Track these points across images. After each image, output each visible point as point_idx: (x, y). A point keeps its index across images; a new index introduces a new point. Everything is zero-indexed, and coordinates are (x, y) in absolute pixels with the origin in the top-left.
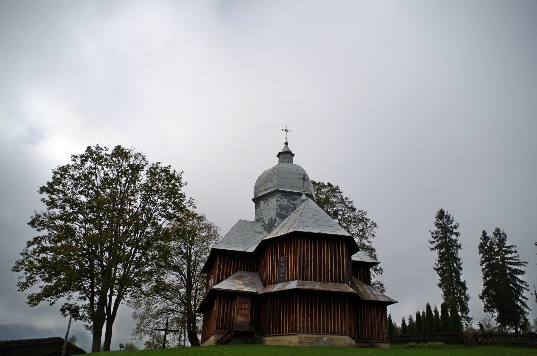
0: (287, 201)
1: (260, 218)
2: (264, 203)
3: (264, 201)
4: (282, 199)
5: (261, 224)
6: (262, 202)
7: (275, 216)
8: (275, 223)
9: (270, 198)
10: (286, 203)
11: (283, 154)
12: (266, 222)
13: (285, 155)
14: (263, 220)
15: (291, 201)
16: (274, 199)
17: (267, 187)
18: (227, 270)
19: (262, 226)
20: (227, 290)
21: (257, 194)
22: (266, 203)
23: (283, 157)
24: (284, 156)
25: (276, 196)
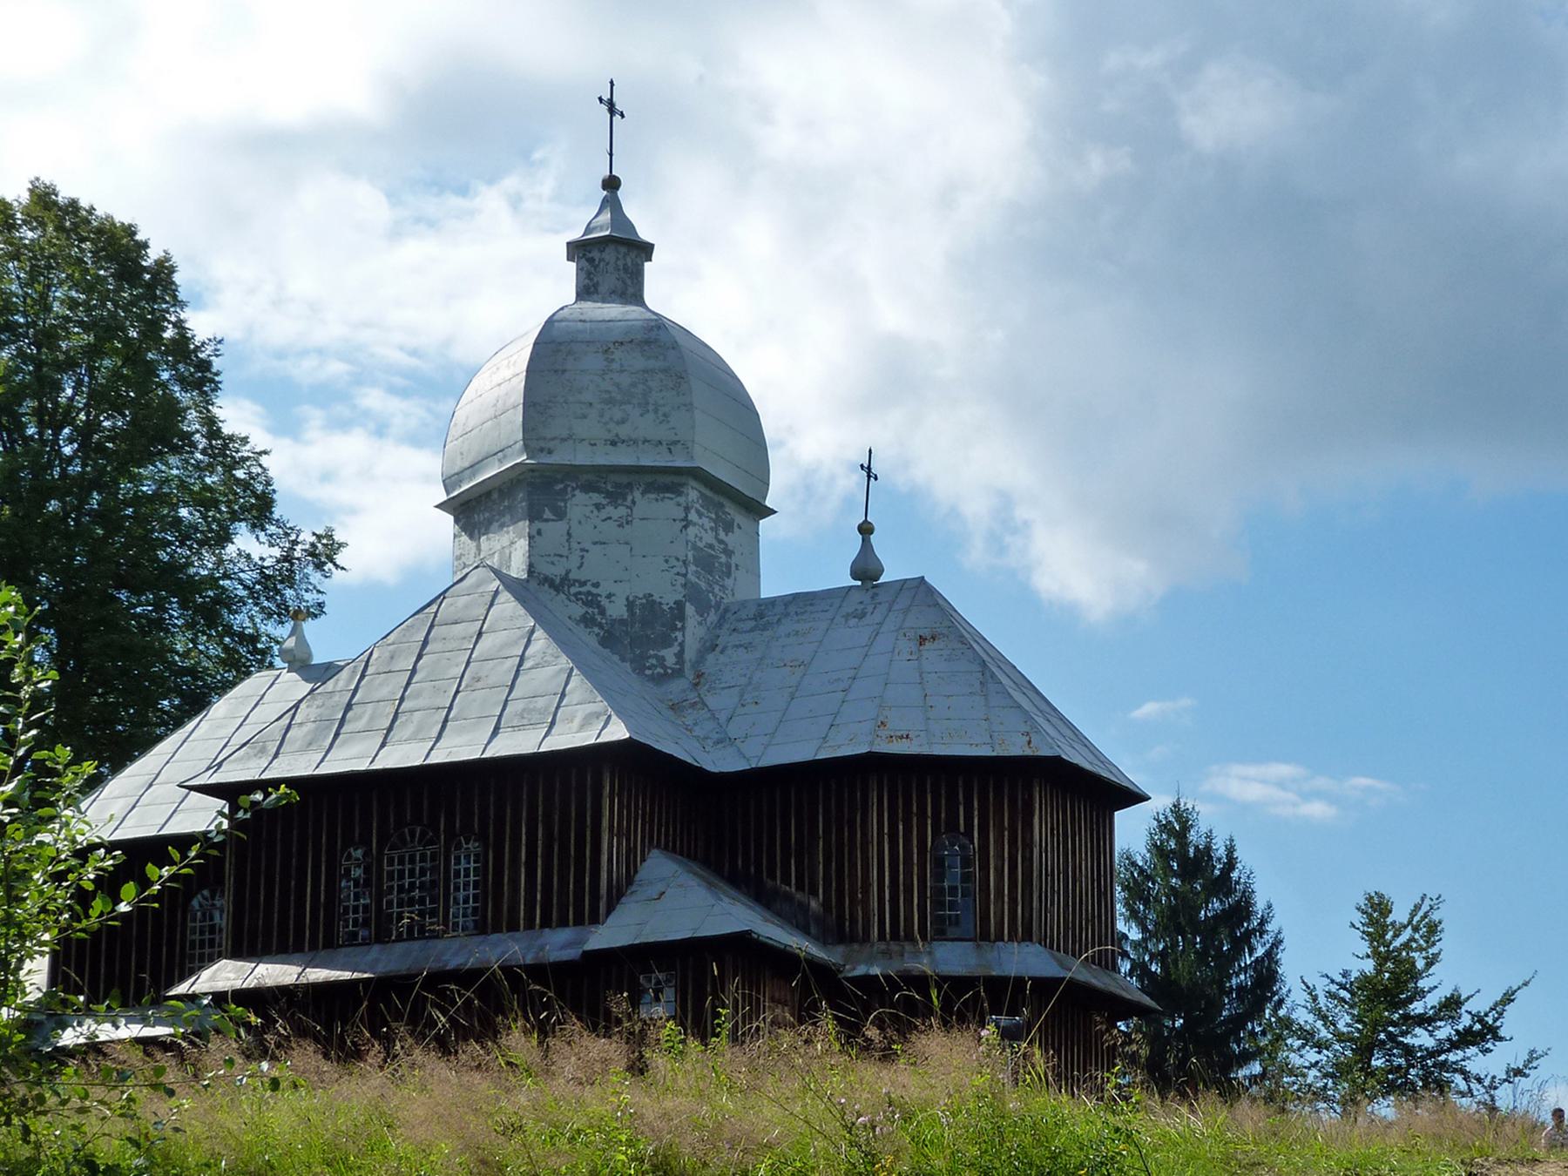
0: (711, 528)
1: (571, 576)
2: (598, 507)
3: (596, 498)
4: (700, 515)
5: (578, 610)
6: (580, 497)
7: (679, 597)
8: (675, 628)
9: (637, 494)
10: (709, 538)
11: (623, 250)
12: (617, 610)
13: (633, 255)
14: (594, 591)
15: (722, 535)
16: (669, 507)
17: (624, 431)
18: (628, 840)
19: (587, 621)
20: (783, 947)
21: (551, 445)
22: (610, 510)
23: (620, 263)
24: (629, 260)
25: (680, 494)
